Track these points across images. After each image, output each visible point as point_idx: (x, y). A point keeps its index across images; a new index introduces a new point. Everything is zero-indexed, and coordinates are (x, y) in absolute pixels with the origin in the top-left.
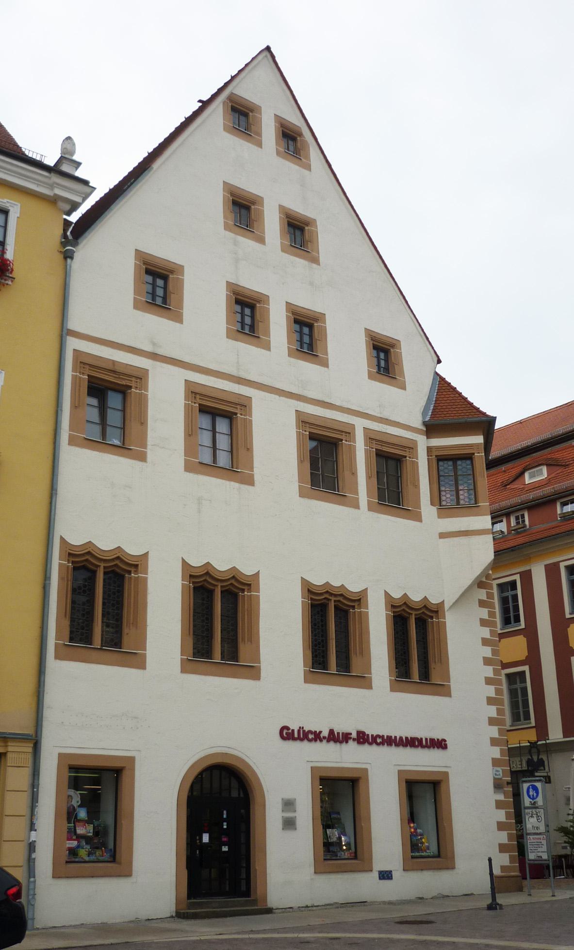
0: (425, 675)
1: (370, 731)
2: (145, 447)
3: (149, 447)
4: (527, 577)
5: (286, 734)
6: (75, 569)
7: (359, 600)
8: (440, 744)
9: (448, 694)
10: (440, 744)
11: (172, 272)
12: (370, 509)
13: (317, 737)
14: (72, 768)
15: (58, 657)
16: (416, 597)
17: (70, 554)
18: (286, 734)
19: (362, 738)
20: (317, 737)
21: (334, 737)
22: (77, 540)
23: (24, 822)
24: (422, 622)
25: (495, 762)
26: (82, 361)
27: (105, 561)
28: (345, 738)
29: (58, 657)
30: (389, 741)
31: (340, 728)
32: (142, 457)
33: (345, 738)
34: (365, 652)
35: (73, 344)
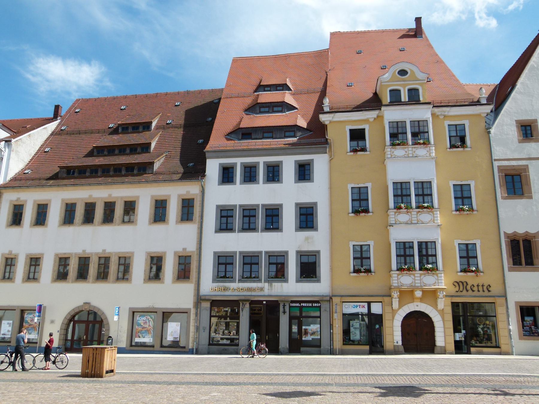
2: (531, 193)
3: (533, 193)
6: (511, 241)
11: (532, 123)
15: (509, 271)
17: (508, 237)
22: (510, 231)
23: (506, 322)
26: (501, 169)
27: (522, 237)
29: (509, 271)
32: (531, 197)
35: (496, 164)
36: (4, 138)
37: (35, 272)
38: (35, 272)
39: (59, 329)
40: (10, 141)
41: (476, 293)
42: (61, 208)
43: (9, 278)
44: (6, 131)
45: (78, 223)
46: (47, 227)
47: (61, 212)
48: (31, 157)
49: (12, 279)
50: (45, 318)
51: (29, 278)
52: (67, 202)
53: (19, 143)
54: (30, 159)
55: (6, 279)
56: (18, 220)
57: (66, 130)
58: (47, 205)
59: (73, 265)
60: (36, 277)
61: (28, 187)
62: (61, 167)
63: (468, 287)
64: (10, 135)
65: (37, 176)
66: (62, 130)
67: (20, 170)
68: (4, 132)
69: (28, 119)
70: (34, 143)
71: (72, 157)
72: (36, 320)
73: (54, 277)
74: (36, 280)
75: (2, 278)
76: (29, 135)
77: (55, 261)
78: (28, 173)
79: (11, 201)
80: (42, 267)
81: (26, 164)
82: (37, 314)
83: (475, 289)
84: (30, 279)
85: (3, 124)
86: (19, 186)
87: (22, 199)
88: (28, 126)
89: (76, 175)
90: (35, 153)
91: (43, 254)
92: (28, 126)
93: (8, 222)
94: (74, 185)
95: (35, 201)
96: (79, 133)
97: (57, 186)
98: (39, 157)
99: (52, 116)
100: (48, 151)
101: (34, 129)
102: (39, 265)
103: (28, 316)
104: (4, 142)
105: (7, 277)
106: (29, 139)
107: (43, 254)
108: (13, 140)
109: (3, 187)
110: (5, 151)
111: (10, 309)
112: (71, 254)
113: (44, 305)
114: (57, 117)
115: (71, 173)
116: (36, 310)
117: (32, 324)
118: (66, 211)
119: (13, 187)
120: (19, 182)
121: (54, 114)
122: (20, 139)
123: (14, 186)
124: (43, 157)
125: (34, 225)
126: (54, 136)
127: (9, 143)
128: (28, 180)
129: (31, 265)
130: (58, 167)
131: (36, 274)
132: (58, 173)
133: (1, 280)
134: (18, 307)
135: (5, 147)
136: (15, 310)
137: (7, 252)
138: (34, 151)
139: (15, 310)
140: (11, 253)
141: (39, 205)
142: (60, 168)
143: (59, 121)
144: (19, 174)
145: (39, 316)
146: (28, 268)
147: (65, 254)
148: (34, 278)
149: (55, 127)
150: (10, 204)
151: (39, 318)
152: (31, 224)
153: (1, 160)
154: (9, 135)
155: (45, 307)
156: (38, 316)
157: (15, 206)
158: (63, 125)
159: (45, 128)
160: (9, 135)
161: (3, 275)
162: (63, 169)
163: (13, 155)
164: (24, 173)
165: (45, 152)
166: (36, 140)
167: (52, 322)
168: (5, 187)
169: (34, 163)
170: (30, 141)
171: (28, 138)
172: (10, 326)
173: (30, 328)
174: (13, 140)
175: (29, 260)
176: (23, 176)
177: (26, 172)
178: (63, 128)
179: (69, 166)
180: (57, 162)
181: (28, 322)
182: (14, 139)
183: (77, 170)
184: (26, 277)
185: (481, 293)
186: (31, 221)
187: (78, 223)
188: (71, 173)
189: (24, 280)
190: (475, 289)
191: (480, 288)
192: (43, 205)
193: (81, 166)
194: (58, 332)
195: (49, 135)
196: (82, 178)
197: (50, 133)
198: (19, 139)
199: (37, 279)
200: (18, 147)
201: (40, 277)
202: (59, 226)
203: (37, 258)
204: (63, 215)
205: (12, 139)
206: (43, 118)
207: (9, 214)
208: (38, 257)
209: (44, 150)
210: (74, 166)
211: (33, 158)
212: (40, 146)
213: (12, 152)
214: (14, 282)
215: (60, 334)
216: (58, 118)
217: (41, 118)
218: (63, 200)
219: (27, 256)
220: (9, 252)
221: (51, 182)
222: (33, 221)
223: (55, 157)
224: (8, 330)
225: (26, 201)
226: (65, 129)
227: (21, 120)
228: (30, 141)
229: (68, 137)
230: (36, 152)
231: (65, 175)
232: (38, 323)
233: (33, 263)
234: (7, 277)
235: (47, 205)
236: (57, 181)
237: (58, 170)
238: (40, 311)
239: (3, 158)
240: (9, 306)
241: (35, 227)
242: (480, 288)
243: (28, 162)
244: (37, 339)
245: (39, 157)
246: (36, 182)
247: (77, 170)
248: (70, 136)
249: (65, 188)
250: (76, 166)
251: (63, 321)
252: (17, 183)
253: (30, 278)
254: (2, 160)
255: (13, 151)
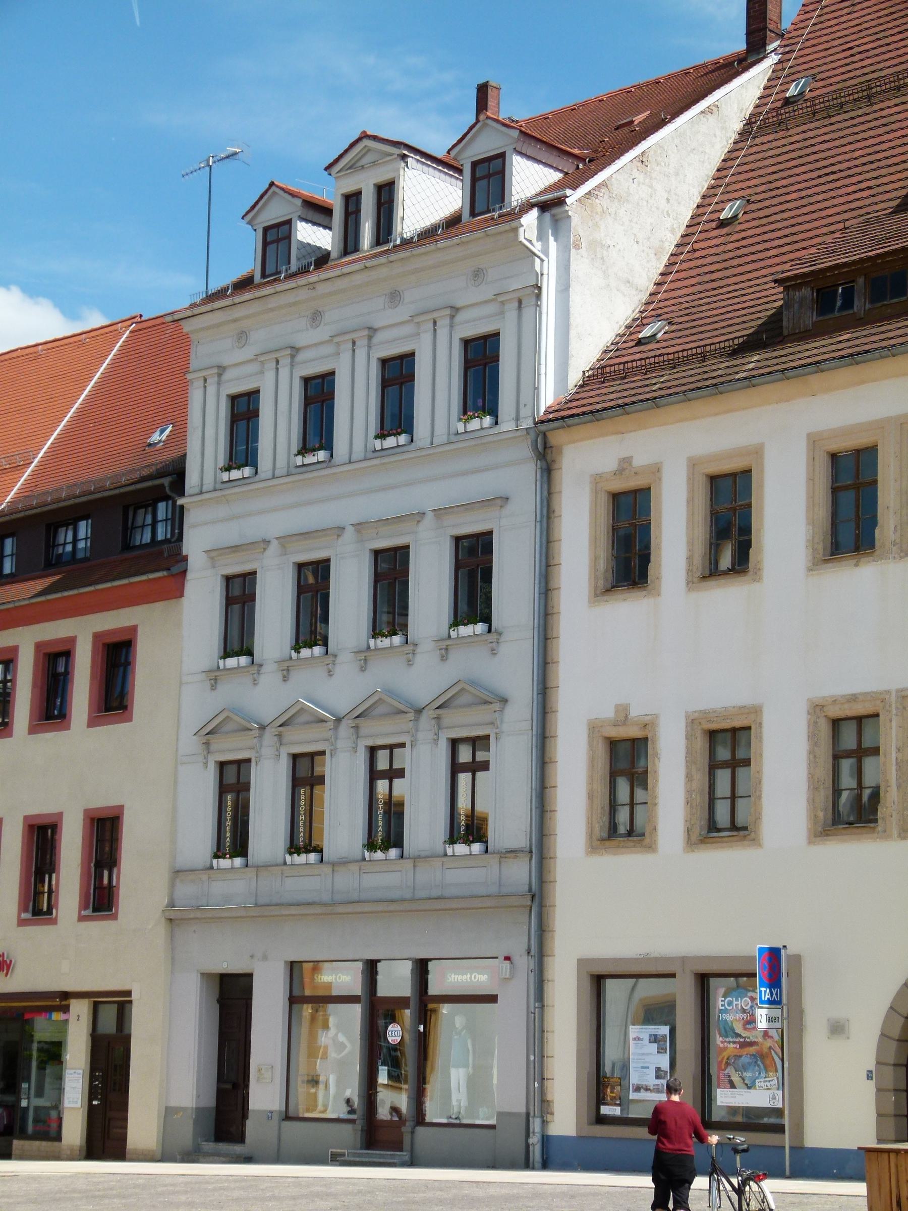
36: (537, 195)
37: (733, 798)
38: (733, 798)
39: (872, 1066)
40: (560, 202)
42: (811, 479)
43: (630, 833)
44: (551, 167)
45: (895, 544)
46: (758, 578)
47: (811, 497)
48: (664, 260)
49: (643, 835)
50: (801, 1012)
51: (713, 827)
52: (836, 446)
53: (603, 201)
54: (661, 268)
55: (621, 836)
56: (635, 563)
57: (808, 95)
58: (747, 473)
59: (898, 750)
60: (740, 821)
61: (654, 402)
62: (788, 279)
64: (560, 175)
65: (691, 344)
66: (787, 102)
67: (621, 331)
68: (536, 165)
69: (639, 87)
70: (669, 192)
71: (841, 226)
72: (762, 1016)
73: (821, 814)
74: (742, 833)
75: (605, 835)
76: (642, 160)
77: (813, 737)
78: (654, 336)
79: (597, 479)
80: (759, 772)
81: (644, 297)
82: (765, 993)
84: (719, 830)
85: (521, 132)
86: (620, 402)
87: (637, 462)
88: (638, 119)
89: (860, 305)
90: (675, 238)
91: (756, 711)
92: (638, 119)
93: (596, 578)
94: (853, 358)
95: (693, 464)
96: (869, 97)
97: (780, 375)
98: (697, 254)
99: (741, 46)
100: (735, 217)
101: (663, 123)
102: (747, 762)
103: (730, 1003)
104: (535, 212)
105: (622, 830)
106: (640, 177)
107: (756, 711)
108: (573, 197)
109: (557, 419)
110: (546, 252)
111: (652, 969)
112: (881, 697)
113: (792, 949)
114: (764, 45)
115: (839, 303)
116: (754, 975)
117: (752, 1039)
118: (836, 491)
119: (595, 414)
120: (617, 386)
121: (749, 34)
122: (604, 184)
123: (599, 407)
124: (712, 251)
125: (704, 578)
126: (757, 141)
127: (555, 211)
128: (657, 367)
129: (713, 766)
130: (775, 281)
131: (741, 804)
132: (779, 312)
133: (602, 840)
134: (684, 960)
135: (541, 236)
136: (673, 975)
137: (609, 713)
138: (673, 231)
139: (673, 975)
140: (626, 717)
141: (714, 480)
142: (786, 289)
143: (773, 59)
144: (615, 349)
145: (774, 1002)
146: (701, 778)
147: (853, 698)
148: (734, 827)
149: (758, 93)
150: (595, 491)
151: (777, 1013)
152: (689, 571)
153: (534, 299)
154: (557, 176)
155: (797, 960)
156: (771, 1002)
157: (616, 497)
158: (791, 78)
159: (709, 110)
160: (557, 176)
161: (606, 819)
162: (798, 287)
163: (580, 265)
164: (640, 342)
165: (723, 224)
166: (677, 174)
167: (837, 1029)
168: (563, 418)
169: (678, 284)
170: (651, 186)
171: (635, 173)
172: (661, 1050)
173: (745, 1060)
174: (573, 197)
175: (701, 744)
176: (637, 354)
177: (647, 332)
178: (793, 91)
179: (821, 270)
180: (777, 260)
181: (733, 1030)
182: (574, 188)
183: (861, 281)
184: (701, 822)
186: (690, 559)
187: (895, 544)
188: (839, 303)
189: (694, 838)
192: (733, 475)
193: (878, 255)
194: (869, 1077)
195: (734, 137)
196: (889, 318)
197: (738, 126)
198: (598, 187)
199: (745, 828)
200: (596, 225)
201: (758, 818)
202: (810, 570)
203: (734, 731)
204: (823, 512)
205: (568, 192)
206: (705, 66)
207: (594, 541)
208: (737, 724)
209: (714, 216)
210: (845, 265)
211: (671, 264)
212: (697, 200)
213: (573, 251)
214: (651, 848)
215: (879, 1090)
216: (770, 48)
217: (697, 68)
218: (813, 441)
219: (692, 722)
220: (616, 712)
221: (753, 360)
222: (698, 560)
223: (765, 237)
224: (658, 1069)
225: (656, 470)
226: (801, 93)
227: (613, 96)
228: (651, 186)
229: (816, 130)
230: (682, 230)
231: (810, 318)
232: (777, 1037)
233: (724, 754)
234: (622, 830)
235: (747, 473)
236: (775, 354)
237: (775, 298)
238: (774, 981)
239: (540, 288)
240: (646, 959)
241: (712, 583)
243: (651, 288)
244: (779, 1112)
245: (697, 254)
246: (691, 373)
247: (861, 281)
248: (826, 122)
249: (815, 380)
250: (854, 263)
251: (882, 1028)
252: (612, 393)
253: (739, 825)
254: (538, 296)
255: (577, 247)
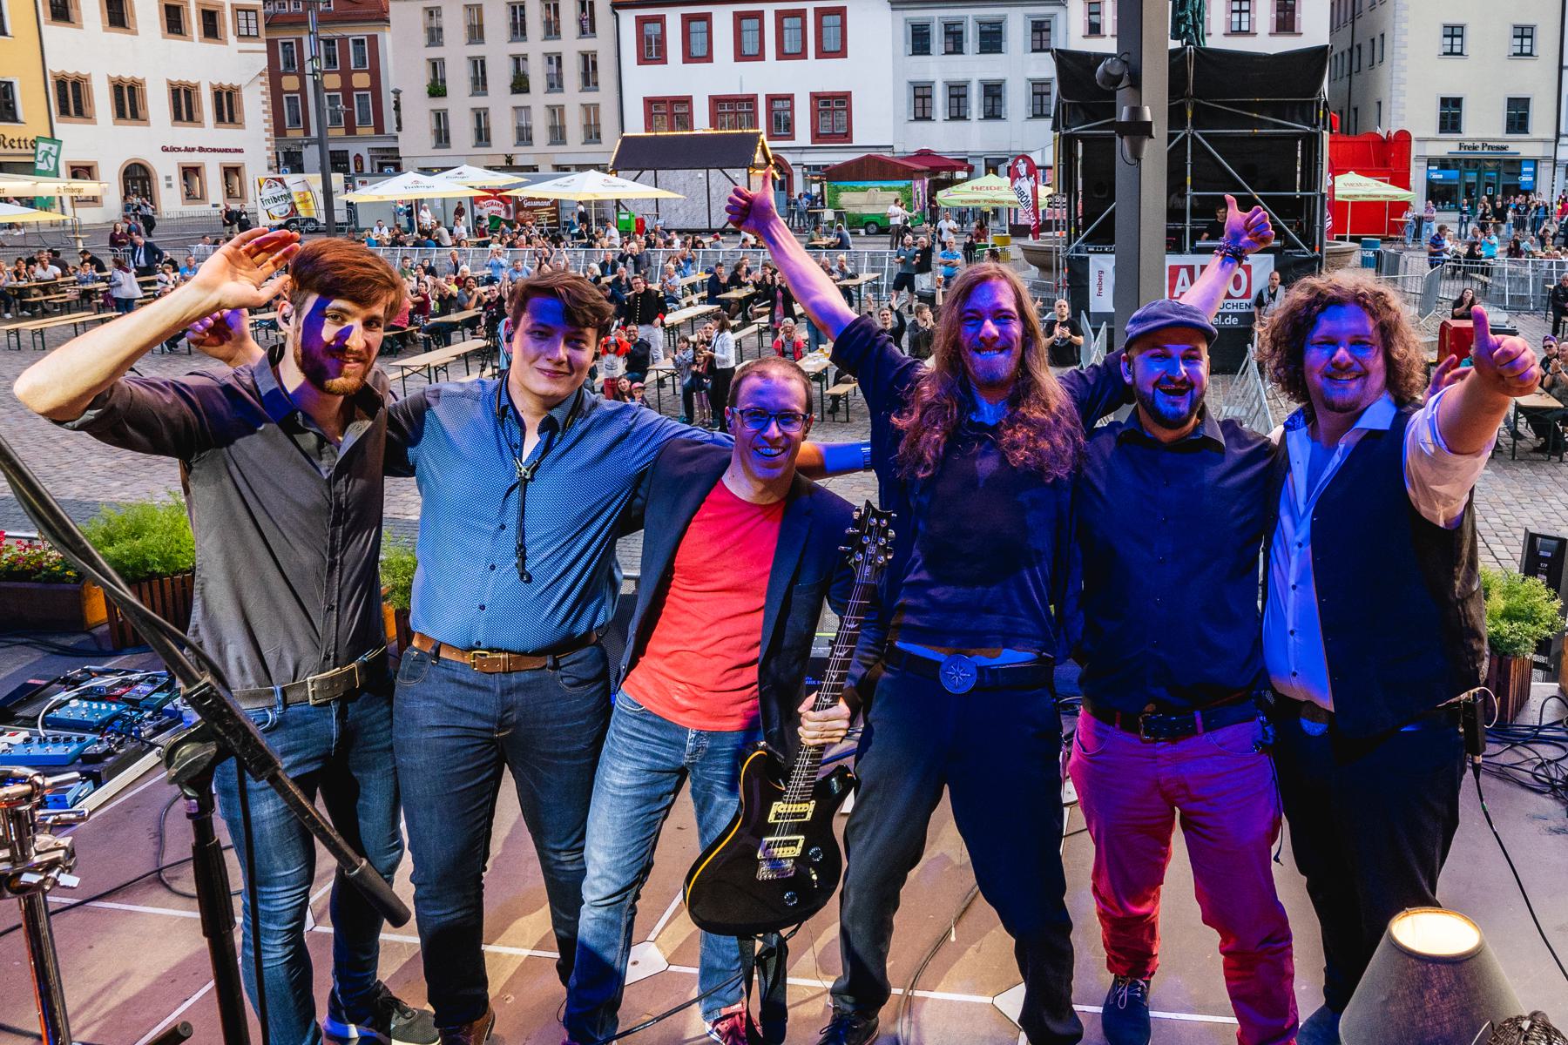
0: (232, 119)
1: (205, 147)
4: (300, 41)
5: (165, 149)
7: (196, 87)
8: (240, 151)
9: (244, 128)
10: (240, 151)
12: (200, 41)
13: (179, 150)
14: (72, 167)
16: (226, 83)
18: (165, 149)
19: (201, 149)
20: (179, 150)
21: (187, 150)
22: (57, 70)
24: (229, 94)
25: (269, 158)
28: (193, 150)
30: (214, 150)
31: (189, 146)
33: (193, 150)
34: (200, 111)
41: (16, 151)
63: (7, 143)
83: (16, 144)
185: (24, 151)
190: (16, 144)
191: (22, 144)
242: (22, 144)
